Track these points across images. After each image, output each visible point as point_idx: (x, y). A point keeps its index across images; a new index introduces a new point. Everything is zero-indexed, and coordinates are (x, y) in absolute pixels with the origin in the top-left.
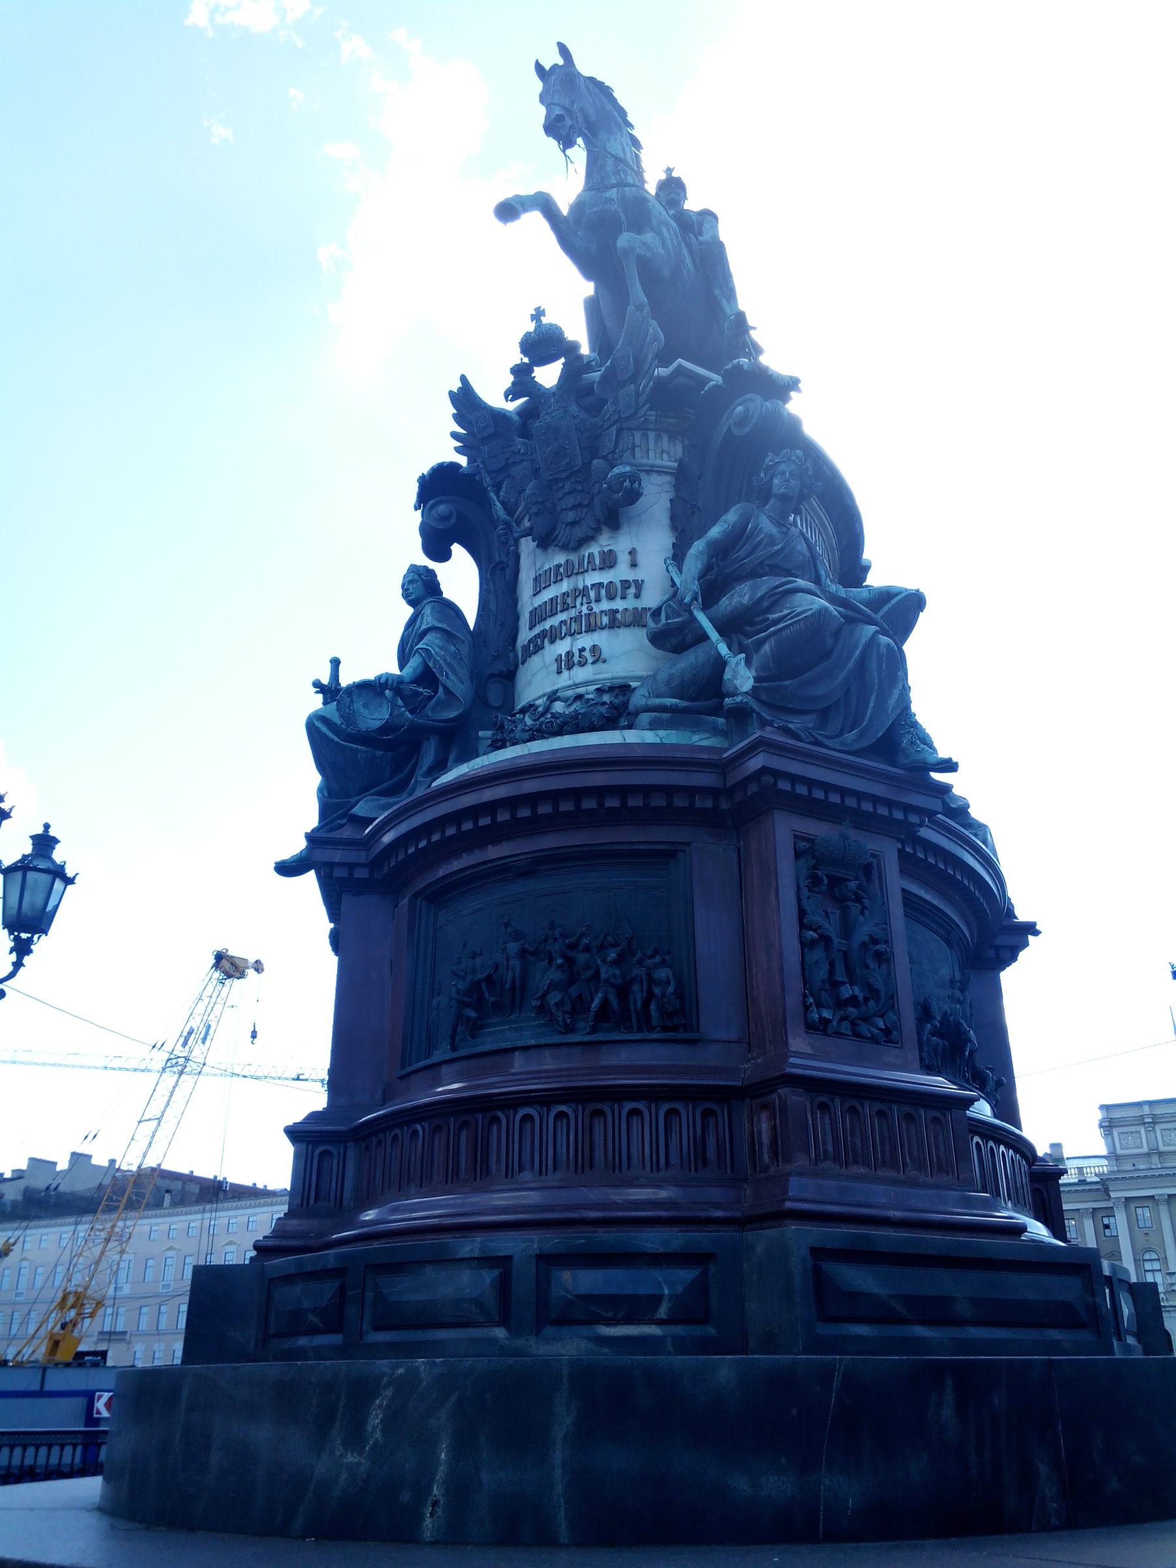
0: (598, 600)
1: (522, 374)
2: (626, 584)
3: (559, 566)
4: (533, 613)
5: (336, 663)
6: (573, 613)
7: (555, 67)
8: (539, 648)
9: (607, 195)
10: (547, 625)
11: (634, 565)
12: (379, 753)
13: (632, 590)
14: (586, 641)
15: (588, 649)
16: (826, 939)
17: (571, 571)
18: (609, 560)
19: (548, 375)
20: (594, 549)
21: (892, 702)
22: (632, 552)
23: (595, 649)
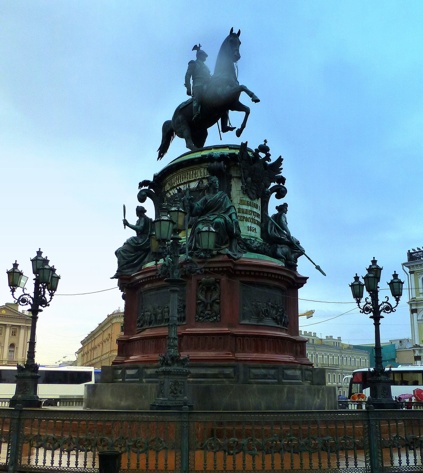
10: (245, 215)
23: (255, 229)
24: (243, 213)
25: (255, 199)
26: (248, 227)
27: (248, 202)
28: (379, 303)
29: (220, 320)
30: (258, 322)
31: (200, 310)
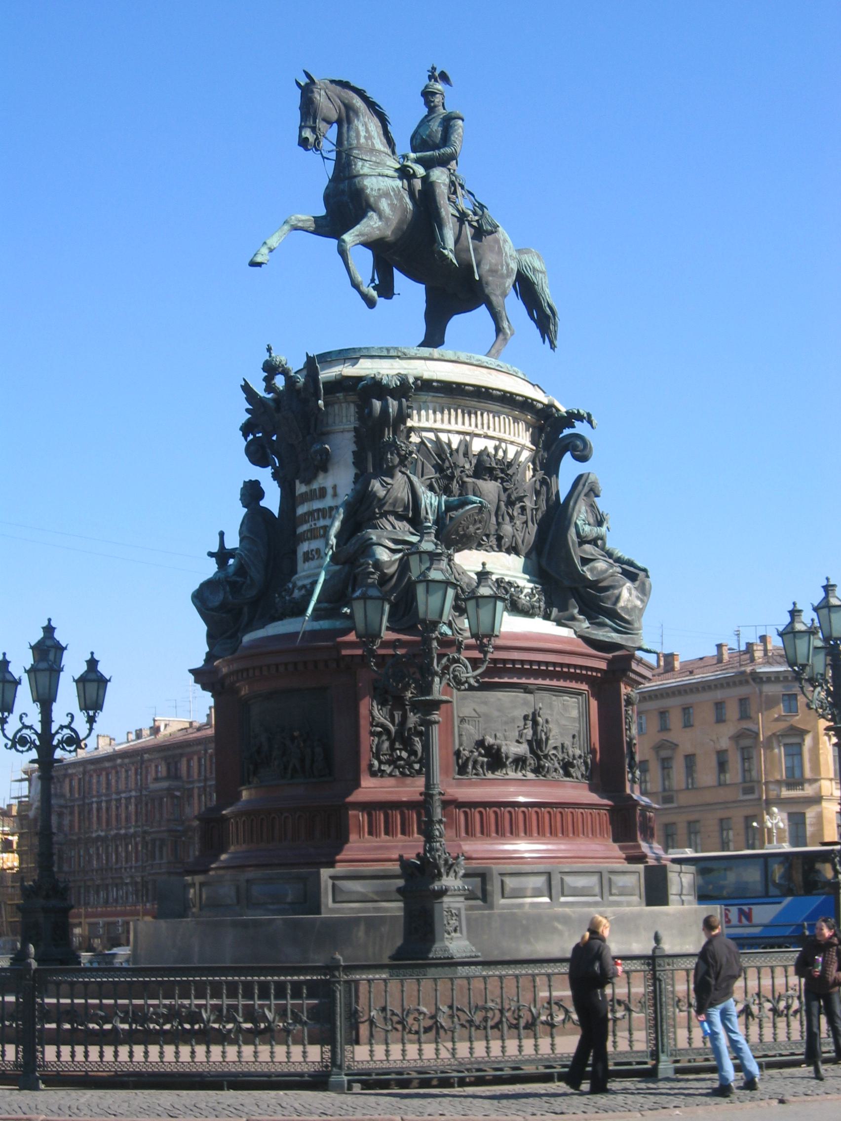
0: (318, 519)
1: (268, 380)
2: (331, 509)
5: (222, 534)
7: (307, 84)
9: (341, 186)
12: (224, 615)
16: (387, 731)
18: (322, 493)
19: (280, 381)
20: (315, 486)
22: (335, 488)
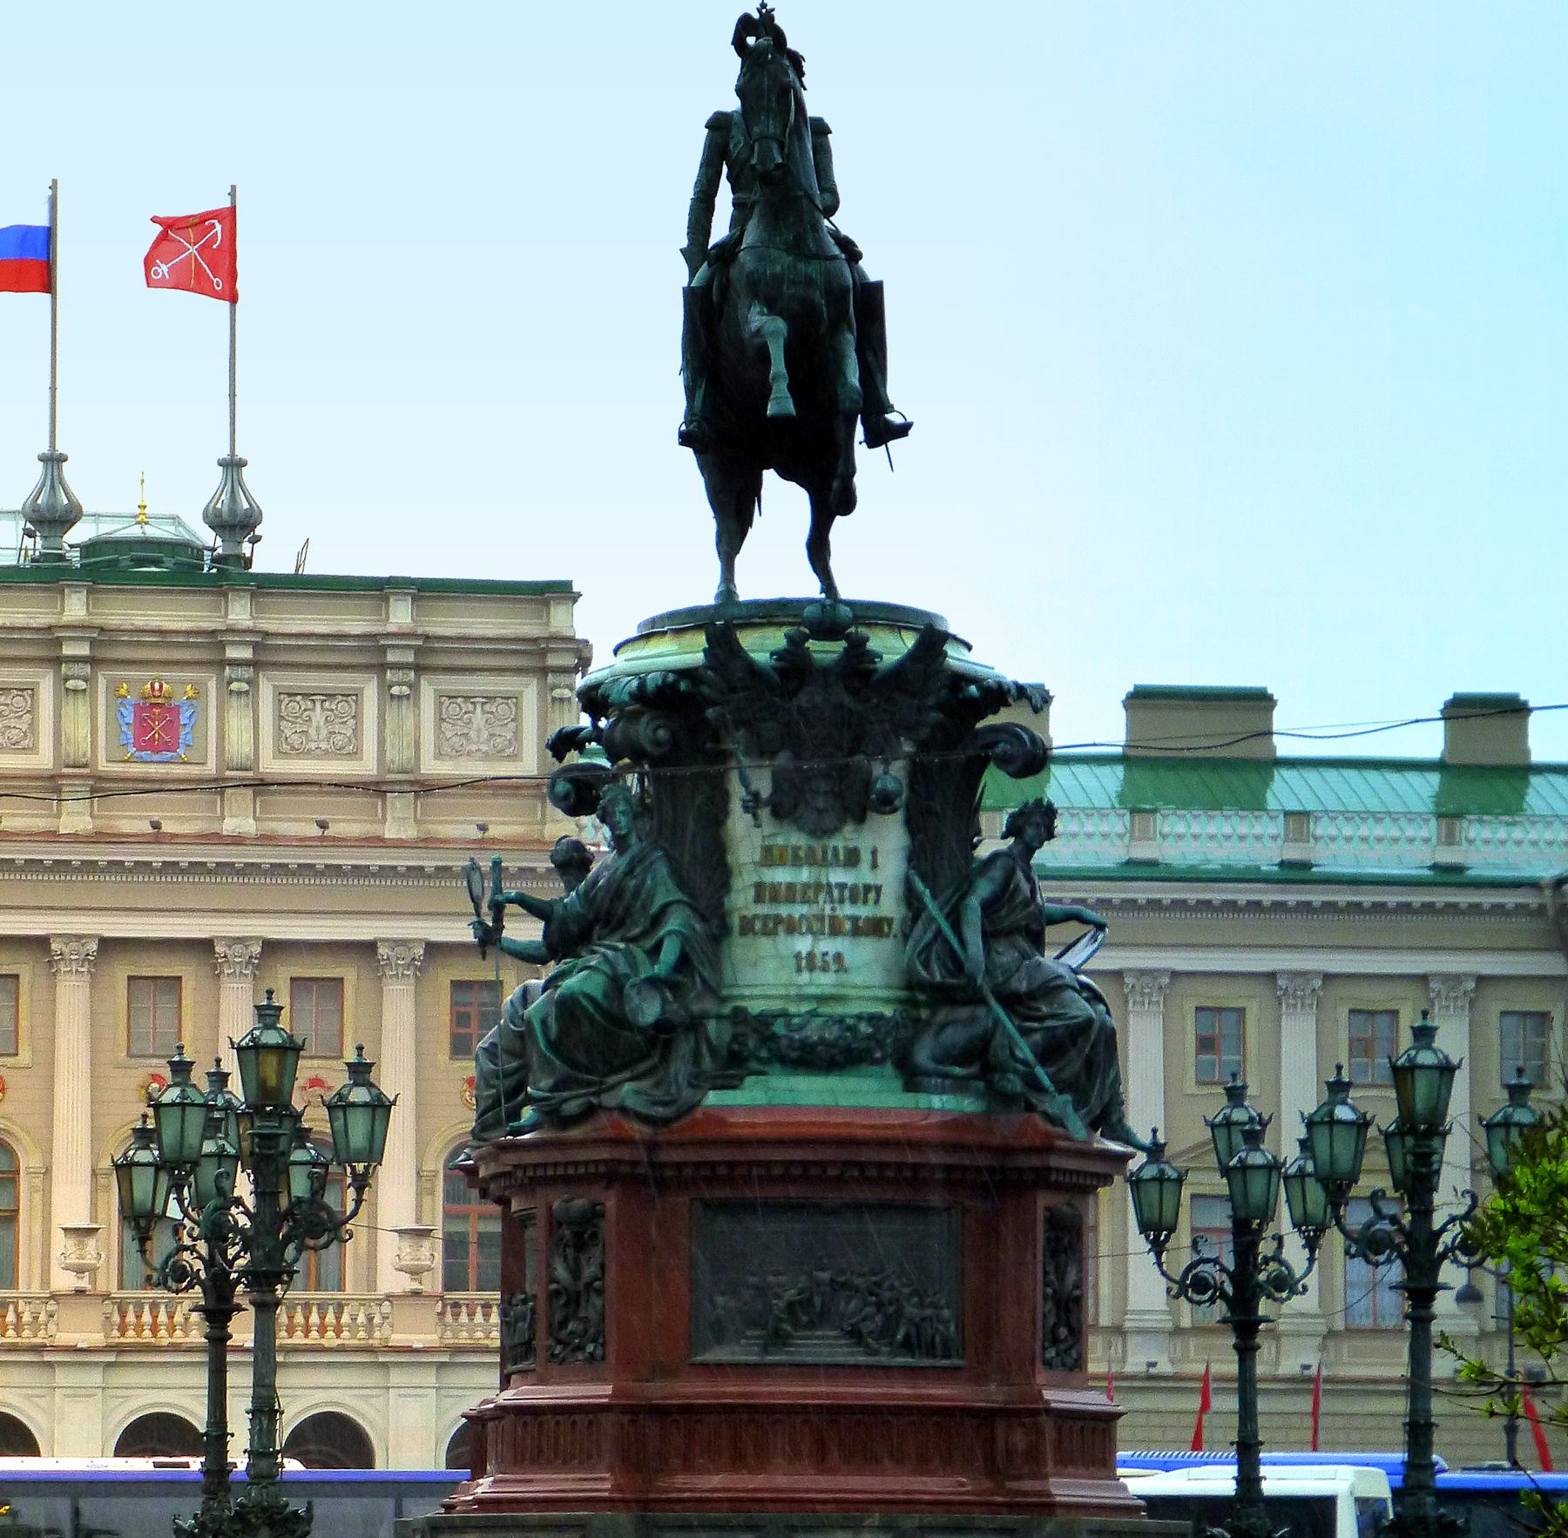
0: (842, 901)
2: (867, 888)
3: (796, 849)
4: (759, 887)
6: (815, 909)
8: (769, 932)
10: (784, 910)
11: (874, 865)
13: (872, 895)
14: (828, 946)
15: (831, 954)
17: (812, 860)
18: (852, 859)
19: (825, 651)
20: (839, 842)
21: (1108, 1082)
22: (874, 853)
23: (838, 957)
24: (774, 899)
25: (836, 830)
26: (798, 956)
27: (800, 848)
28: (1438, 1221)
29: (603, 1358)
30: (765, 1350)
31: (558, 1317)
